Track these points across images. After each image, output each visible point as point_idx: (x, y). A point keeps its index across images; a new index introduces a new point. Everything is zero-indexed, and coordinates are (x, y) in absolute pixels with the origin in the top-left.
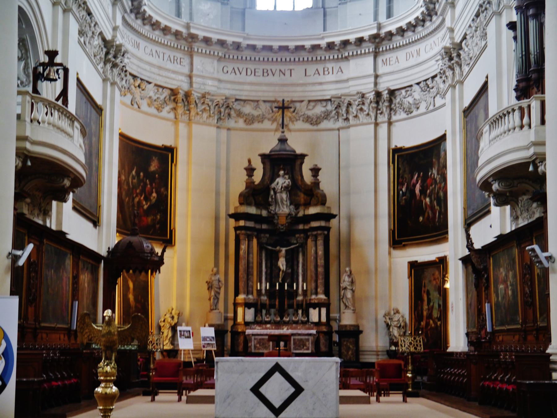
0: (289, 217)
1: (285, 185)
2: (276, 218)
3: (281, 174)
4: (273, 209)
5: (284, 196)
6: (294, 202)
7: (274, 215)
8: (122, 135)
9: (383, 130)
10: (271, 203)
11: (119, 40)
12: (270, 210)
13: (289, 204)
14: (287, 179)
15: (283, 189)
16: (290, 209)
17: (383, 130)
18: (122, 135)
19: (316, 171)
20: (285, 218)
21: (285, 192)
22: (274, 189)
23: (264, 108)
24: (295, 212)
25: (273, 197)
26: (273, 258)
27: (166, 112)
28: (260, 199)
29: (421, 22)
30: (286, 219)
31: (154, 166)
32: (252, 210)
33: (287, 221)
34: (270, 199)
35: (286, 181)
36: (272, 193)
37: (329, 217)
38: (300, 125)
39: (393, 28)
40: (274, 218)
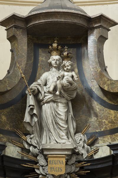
0: (74, 159)
1: (64, 81)
2: (41, 161)
3: (53, 62)
4: (34, 142)
5: (61, 109)
7: (36, 156)
10: (29, 129)
12: (26, 146)
13: (72, 131)
14: (68, 71)
15: (58, 93)
16: (75, 141)
20: (64, 160)
21: (64, 101)
22: (36, 94)
24: (88, 151)
25: (35, 112)
28: (4, 118)
30: (66, 164)
33: (69, 171)
34: (27, 118)
35: (66, 73)
36: (31, 101)
40: (36, 163)
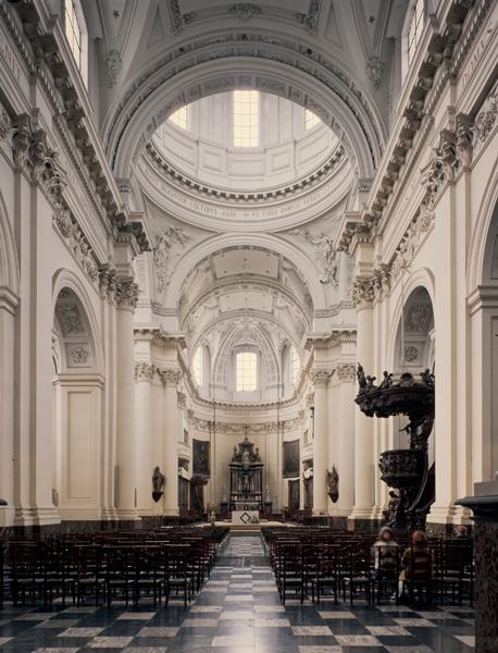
6: (250, 460)
8: (194, 440)
9: (280, 436)
11: (193, 409)
17: (280, 436)
18: (194, 440)
19: (257, 450)
23: (239, 427)
26: (243, 478)
27: (207, 429)
29: (293, 399)
31: (203, 448)
32: (235, 463)
37: (262, 465)
38: (252, 432)
39: (283, 400)
